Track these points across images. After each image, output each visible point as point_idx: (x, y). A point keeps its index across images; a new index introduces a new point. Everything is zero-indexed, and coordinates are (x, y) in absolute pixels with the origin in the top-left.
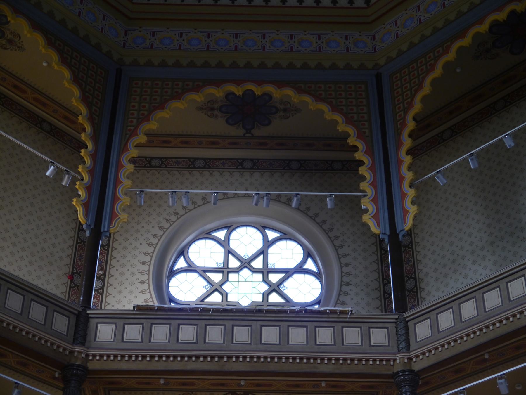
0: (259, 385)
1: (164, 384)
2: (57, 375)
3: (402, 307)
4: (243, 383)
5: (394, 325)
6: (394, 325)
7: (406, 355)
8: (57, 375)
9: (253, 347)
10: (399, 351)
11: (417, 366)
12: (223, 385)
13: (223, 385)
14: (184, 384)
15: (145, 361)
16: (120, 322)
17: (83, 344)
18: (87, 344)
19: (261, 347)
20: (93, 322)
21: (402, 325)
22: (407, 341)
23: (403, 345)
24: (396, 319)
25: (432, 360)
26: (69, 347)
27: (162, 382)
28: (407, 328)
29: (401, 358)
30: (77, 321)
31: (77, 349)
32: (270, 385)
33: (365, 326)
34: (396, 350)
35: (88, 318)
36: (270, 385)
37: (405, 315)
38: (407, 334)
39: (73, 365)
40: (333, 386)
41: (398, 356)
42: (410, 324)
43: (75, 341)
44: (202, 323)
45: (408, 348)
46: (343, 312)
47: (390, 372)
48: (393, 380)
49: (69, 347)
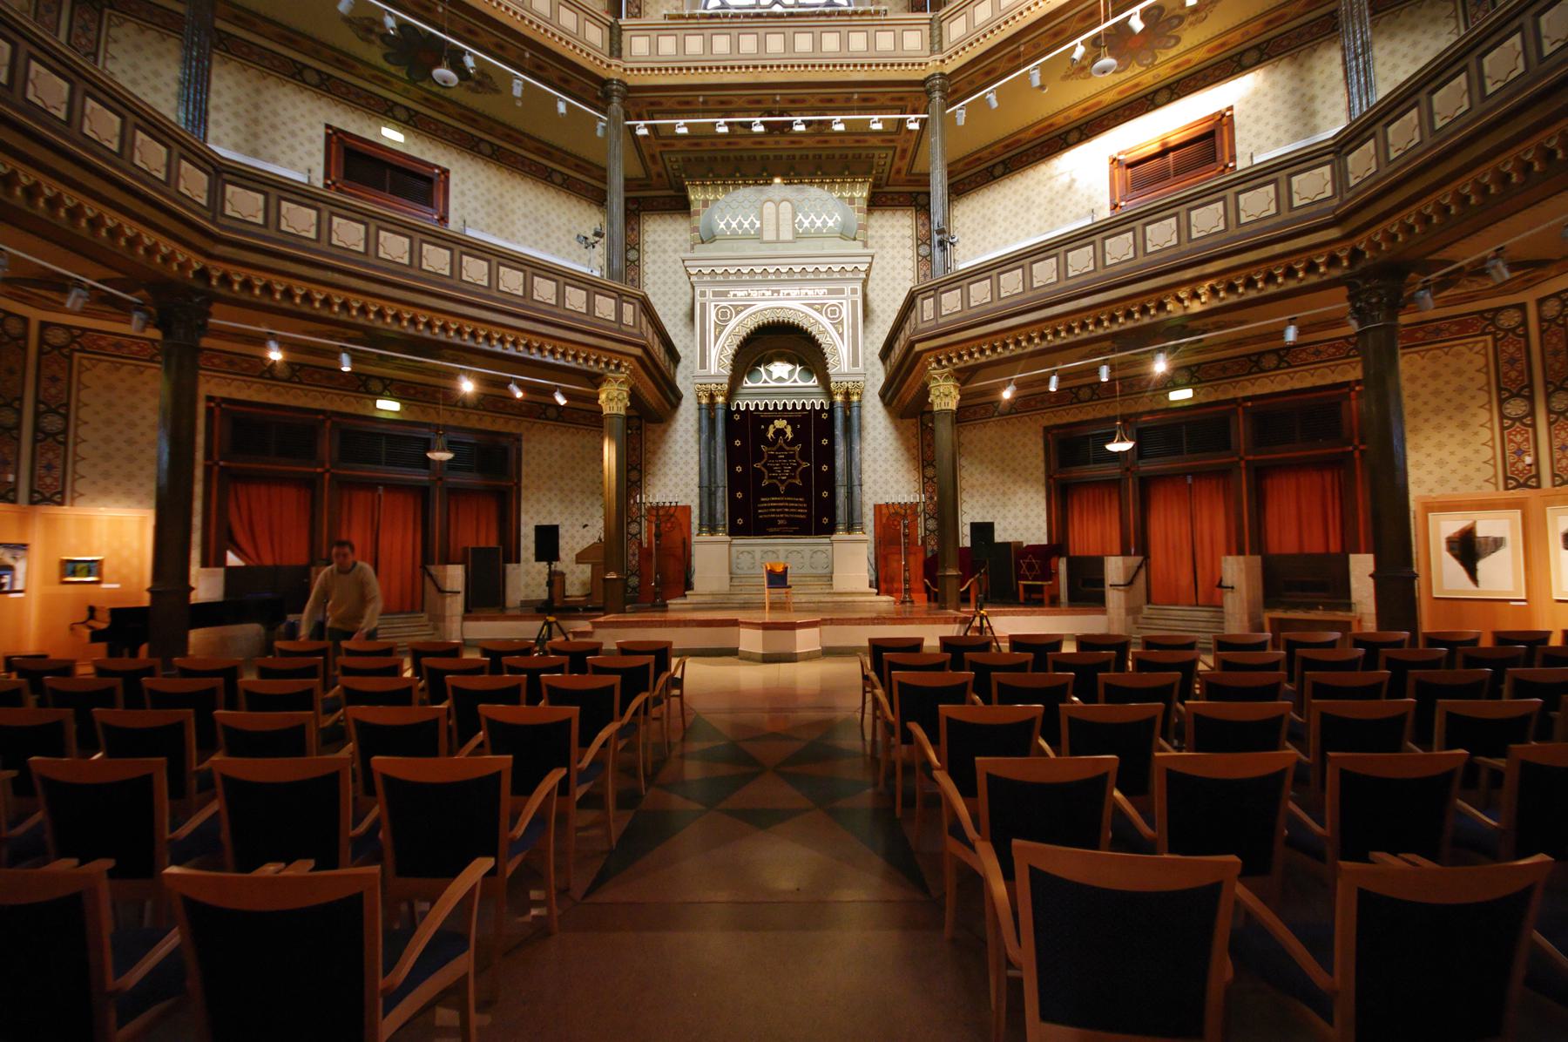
0: (793, 101)
1: (705, 103)
2: (599, 94)
3: (936, 6)
4: (778, 98)
5: (928, 27)
6: (928, 27)
7: (939, 57)
8: (599, 94)
9: (786, 56)
10: (932, 52)
11: (949, 68)
12: (759, 102)
13: (759, 102)
14: (722, 103)
15: (681, 75)
16: (654, 34)
17: (620, 57)
18: (623, 58)
19: (794, 55)
20: (626, 36)
21: (936, 25)
22: (941, 41)
23: (936, 47)
24: (931, 19)
25: (965, 58)
26: (607, 60)
27: (701, 99)
28: (940, 28)
29: (933, 66)
30: (611, 33)
31: (614, 62)
32: (803, 101)
33: (898, 29)
34: (928, 53)
35: (620, 30)
36: (803, 101)
37: (941, 13)
38: (941, 35)
39: (612, 80)
40: (865, 100)
41: (928, 60)
42: (945, 24)
43: (611, 55)
44: (734, 32)
45: (941, 50)
46: (877, 13)
47: (922, 78)
48: (922, 89)
49: (607, 60)
